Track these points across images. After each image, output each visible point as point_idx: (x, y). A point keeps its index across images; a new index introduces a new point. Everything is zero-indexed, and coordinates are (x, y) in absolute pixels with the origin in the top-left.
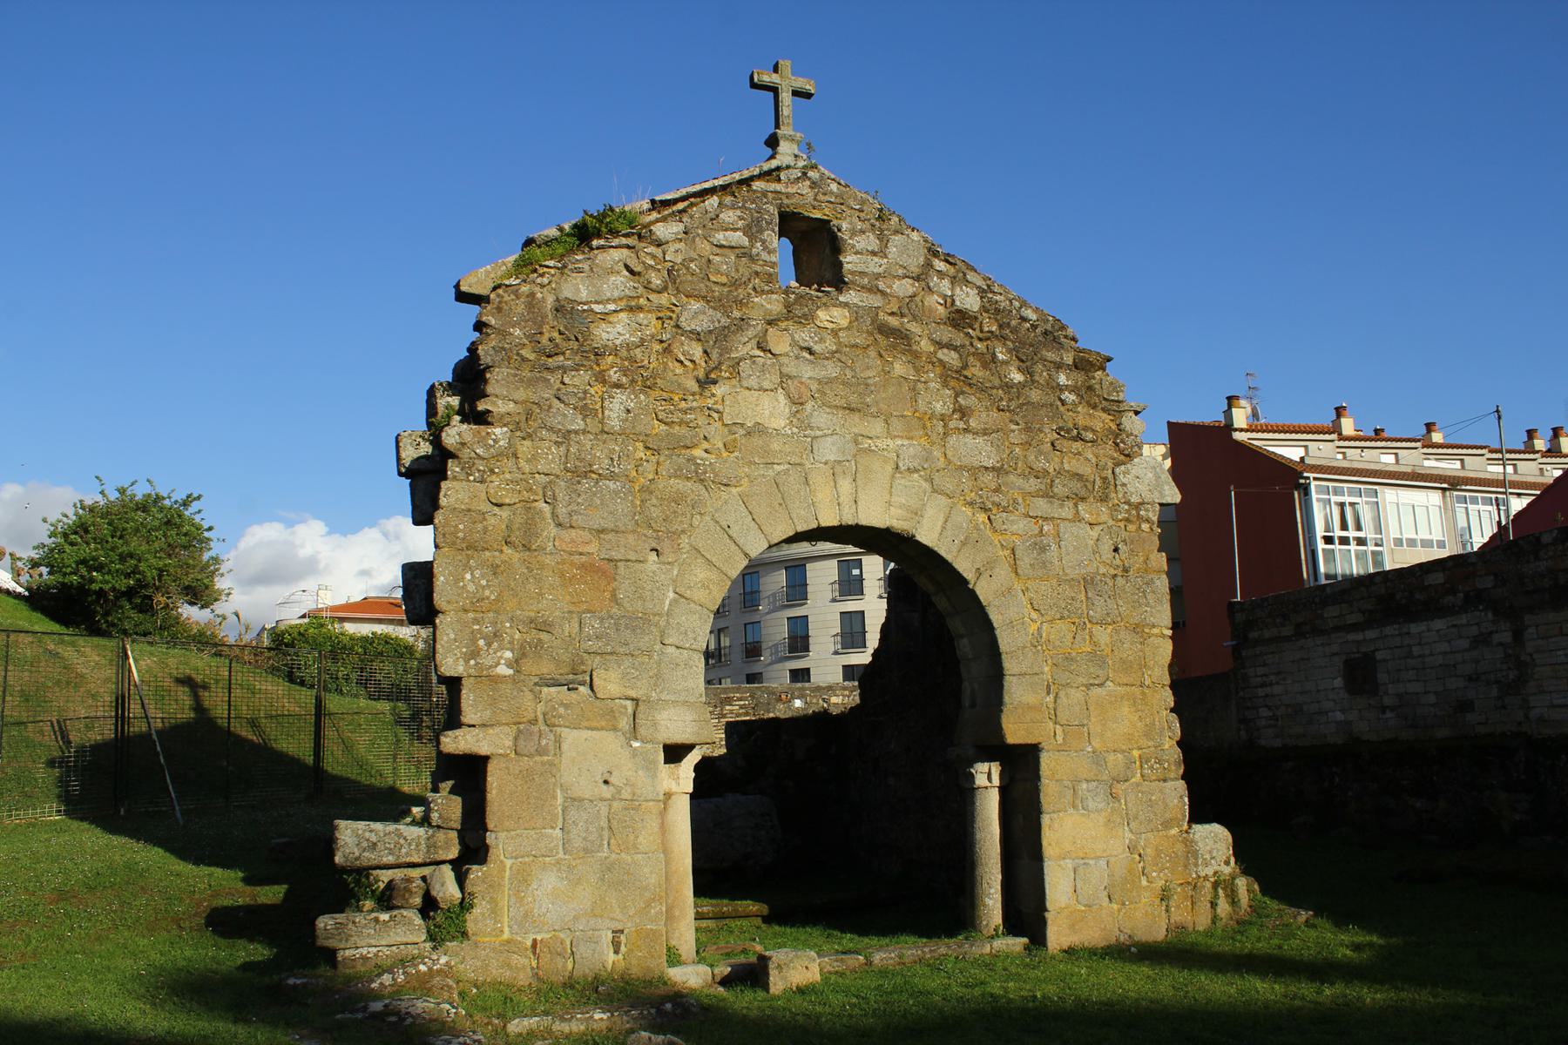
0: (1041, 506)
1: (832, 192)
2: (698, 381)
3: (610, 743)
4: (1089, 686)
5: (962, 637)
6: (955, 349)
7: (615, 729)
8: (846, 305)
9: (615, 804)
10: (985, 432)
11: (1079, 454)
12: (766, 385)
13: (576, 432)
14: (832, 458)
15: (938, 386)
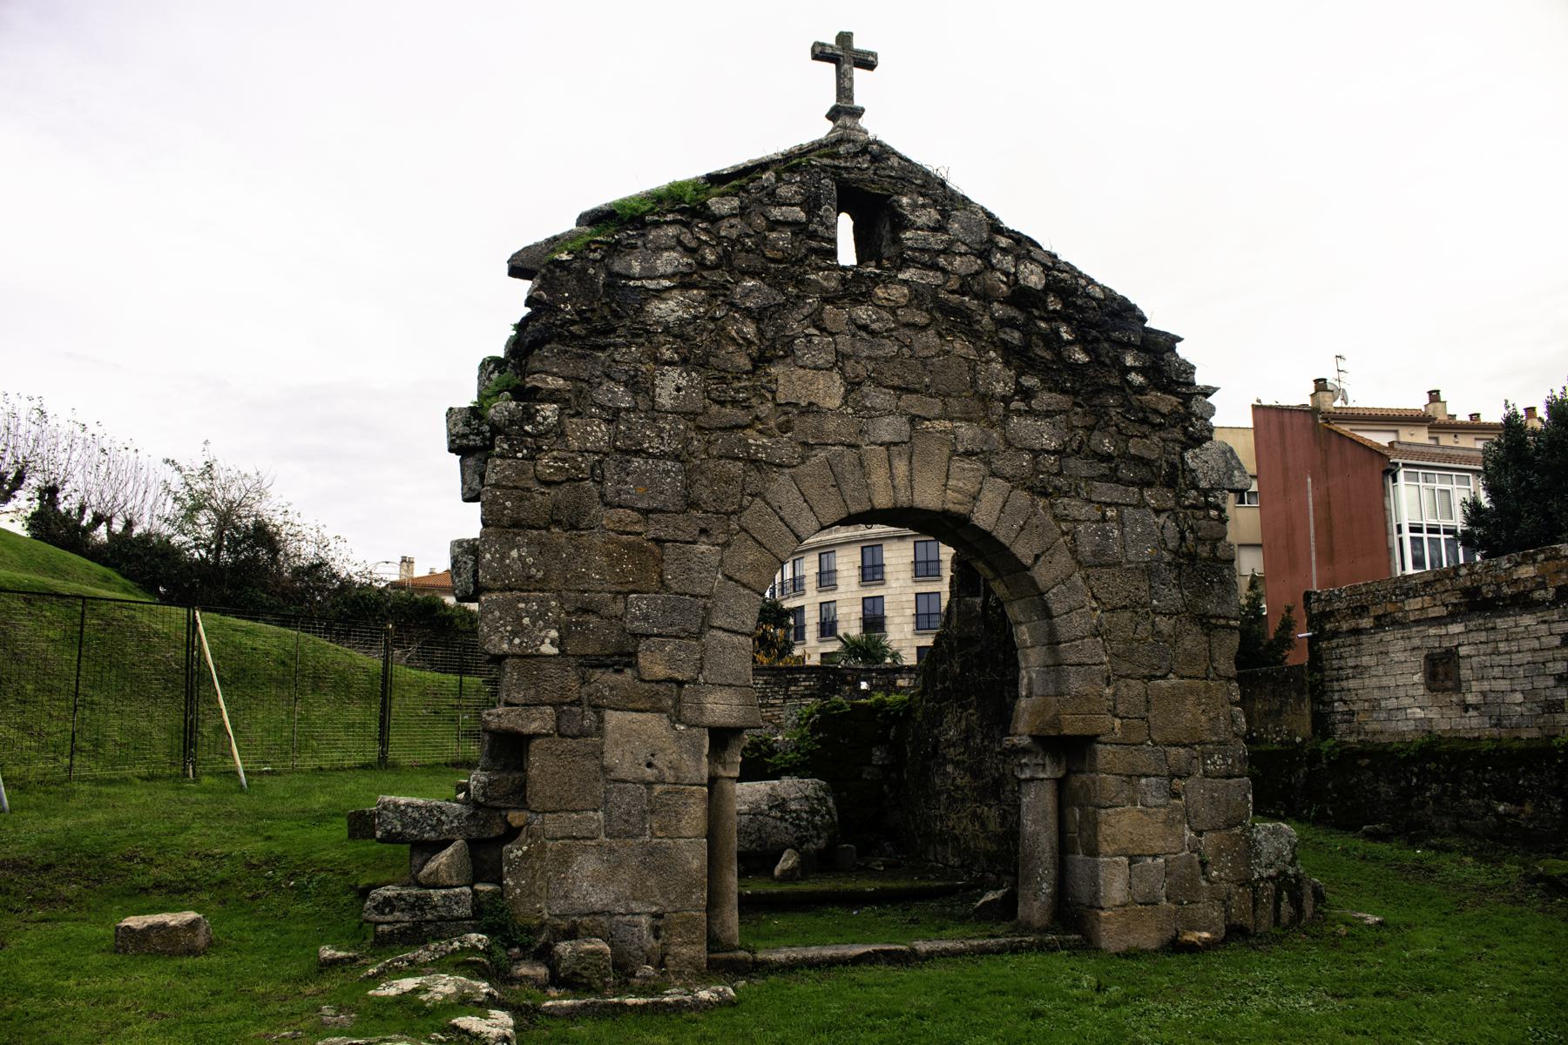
0: (1105, 492)
1: (892, 168)
2: (752, 359)
3: (655, 724)
4: (1151, 678)
5: (1020, 623)
7: (660, 711)
8: (905, 282)
9: (658, 788)
10: (1048, 414)
13: (627, 410)
14: (887, 438)
15: (999, 367)
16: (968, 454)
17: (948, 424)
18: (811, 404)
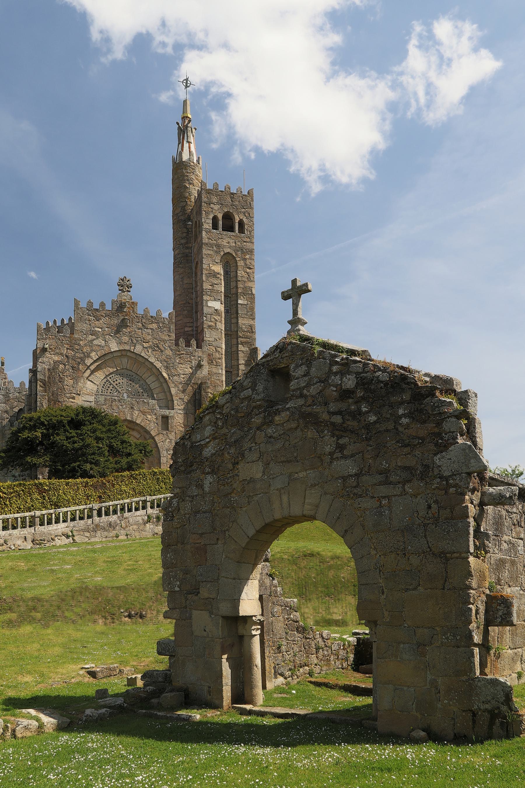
0: (383, 490)
6: (339, 413)
10: (352, 456)
11: (409, 454)
12: (254, 459)
14: (279, 487)
16: (313, 486)
17: (305, 474)
18: (251, 478)
